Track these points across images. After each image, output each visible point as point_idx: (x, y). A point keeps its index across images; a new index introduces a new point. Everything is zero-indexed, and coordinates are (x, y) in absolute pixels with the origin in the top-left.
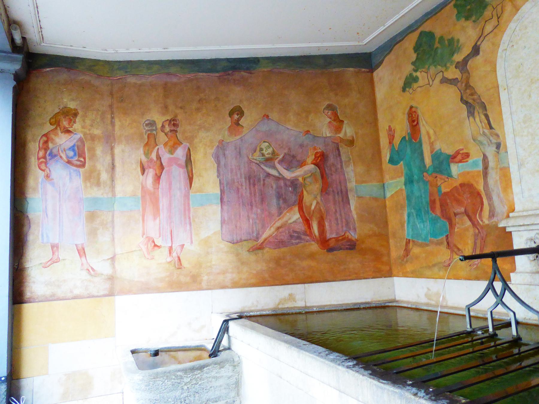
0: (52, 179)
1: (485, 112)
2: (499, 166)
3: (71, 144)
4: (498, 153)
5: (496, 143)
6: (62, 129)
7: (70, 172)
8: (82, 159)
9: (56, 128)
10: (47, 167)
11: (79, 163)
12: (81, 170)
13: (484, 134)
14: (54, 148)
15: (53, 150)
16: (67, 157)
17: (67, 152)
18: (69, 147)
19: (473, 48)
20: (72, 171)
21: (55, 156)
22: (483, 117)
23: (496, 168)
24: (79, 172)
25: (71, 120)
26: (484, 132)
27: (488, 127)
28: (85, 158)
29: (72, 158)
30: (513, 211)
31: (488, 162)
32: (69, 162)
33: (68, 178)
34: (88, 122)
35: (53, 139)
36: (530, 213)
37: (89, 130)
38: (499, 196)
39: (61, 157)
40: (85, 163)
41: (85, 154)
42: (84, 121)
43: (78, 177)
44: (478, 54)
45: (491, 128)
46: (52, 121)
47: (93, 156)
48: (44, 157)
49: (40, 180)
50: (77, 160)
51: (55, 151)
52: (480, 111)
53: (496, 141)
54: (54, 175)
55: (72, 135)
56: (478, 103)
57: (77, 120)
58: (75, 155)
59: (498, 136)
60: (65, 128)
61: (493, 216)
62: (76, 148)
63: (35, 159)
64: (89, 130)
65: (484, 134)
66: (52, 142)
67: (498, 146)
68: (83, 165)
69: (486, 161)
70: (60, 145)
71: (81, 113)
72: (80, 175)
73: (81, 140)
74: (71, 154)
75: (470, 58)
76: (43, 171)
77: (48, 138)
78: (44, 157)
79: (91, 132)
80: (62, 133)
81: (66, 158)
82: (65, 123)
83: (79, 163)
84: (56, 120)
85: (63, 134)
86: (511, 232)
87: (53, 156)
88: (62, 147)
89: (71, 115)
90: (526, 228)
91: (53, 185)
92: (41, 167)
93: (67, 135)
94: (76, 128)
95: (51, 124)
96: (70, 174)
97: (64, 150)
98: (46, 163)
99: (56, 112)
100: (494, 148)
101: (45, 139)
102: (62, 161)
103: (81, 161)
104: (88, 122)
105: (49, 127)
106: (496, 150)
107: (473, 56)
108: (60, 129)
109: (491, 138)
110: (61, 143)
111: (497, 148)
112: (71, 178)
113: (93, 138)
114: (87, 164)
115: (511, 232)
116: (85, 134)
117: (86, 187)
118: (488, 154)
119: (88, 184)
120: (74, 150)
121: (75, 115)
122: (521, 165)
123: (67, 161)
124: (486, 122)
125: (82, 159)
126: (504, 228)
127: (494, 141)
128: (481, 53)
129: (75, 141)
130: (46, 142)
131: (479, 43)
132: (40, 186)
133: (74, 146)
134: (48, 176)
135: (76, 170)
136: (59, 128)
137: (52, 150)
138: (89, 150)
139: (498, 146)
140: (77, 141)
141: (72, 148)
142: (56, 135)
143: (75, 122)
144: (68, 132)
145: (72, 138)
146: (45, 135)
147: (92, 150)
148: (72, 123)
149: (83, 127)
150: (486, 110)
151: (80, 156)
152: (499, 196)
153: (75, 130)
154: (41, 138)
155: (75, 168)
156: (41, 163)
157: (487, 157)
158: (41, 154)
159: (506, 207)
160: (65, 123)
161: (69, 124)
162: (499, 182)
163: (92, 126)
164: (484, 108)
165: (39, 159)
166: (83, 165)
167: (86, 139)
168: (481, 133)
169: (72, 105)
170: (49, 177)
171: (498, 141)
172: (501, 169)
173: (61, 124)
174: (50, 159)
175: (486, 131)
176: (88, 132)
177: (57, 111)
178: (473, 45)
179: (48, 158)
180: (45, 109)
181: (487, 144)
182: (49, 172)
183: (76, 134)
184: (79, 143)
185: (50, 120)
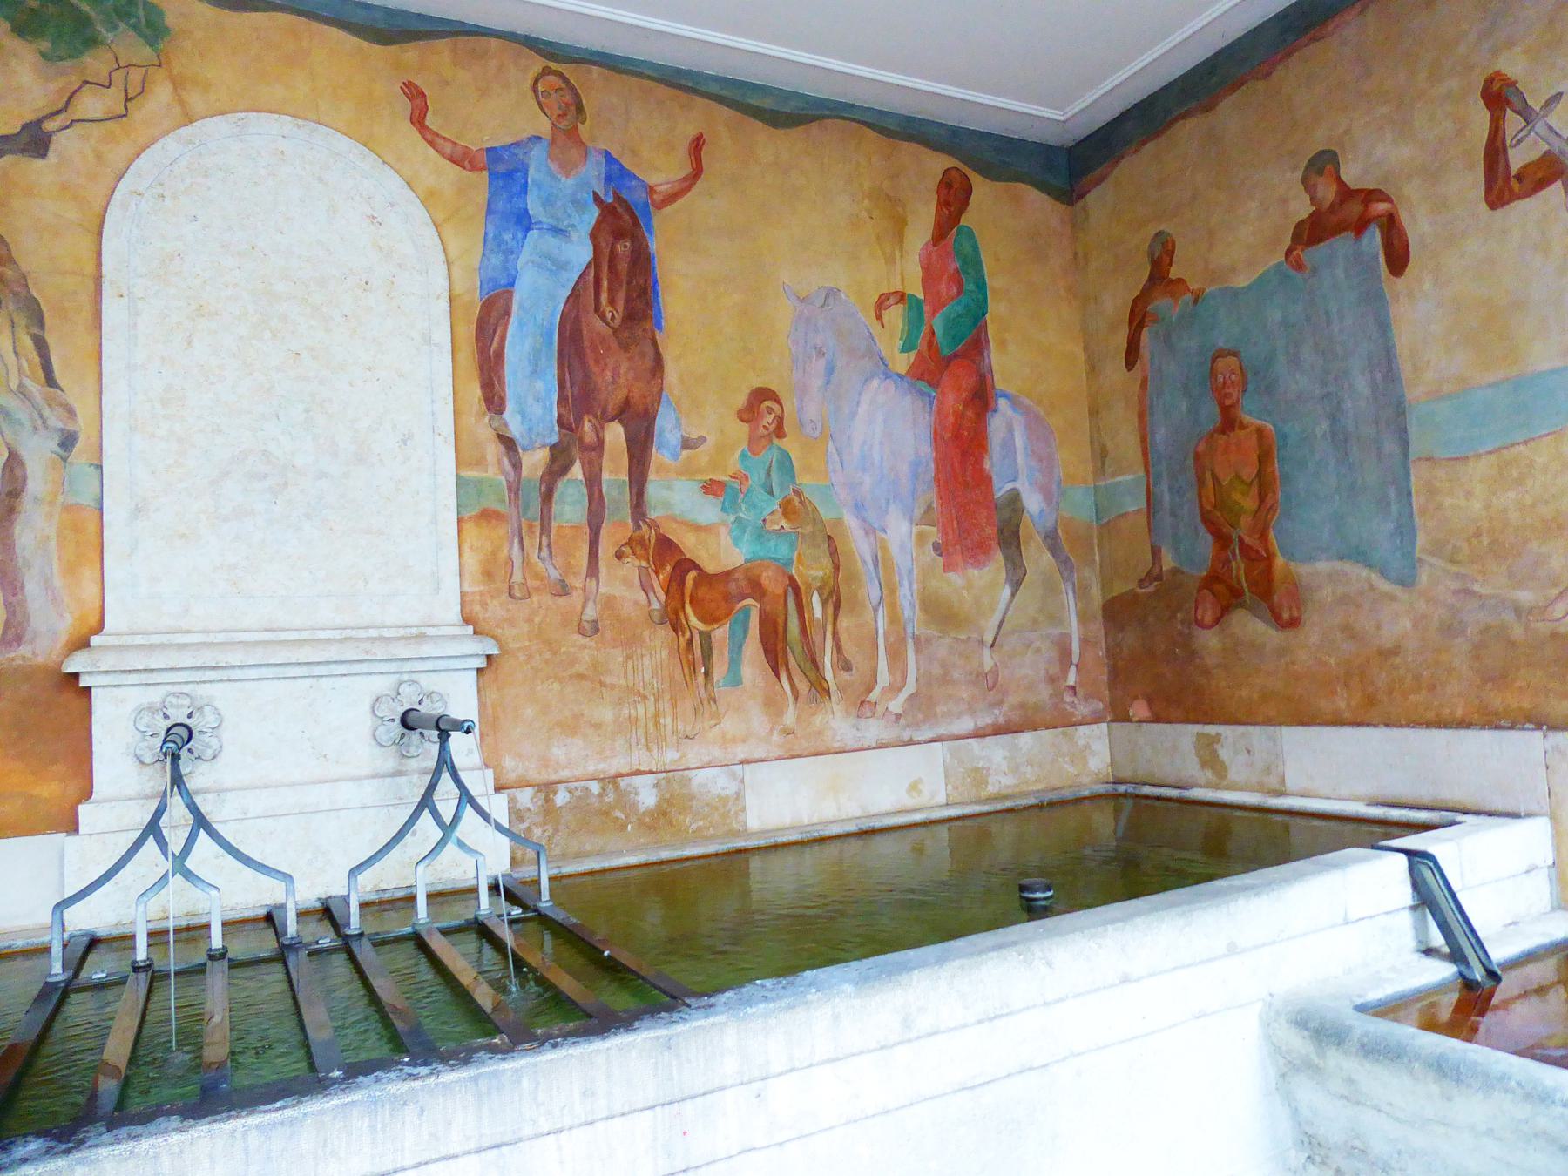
1: (35, 330)
2: (61, 499)
4: (65, 460)
5: (62, 430)
13: (22, 391)
19: (25, 127)
22: (28, 343)
23: (51, 503)
26: (21, 385)
27: (41, 374)
30: (99, 628)
31: (25, 479)
36: (155, 639)
38: (47, 584)
44: (43, 155)
45: (50, 381)
52: (21, 321)
53: (60, 425)
56: (15, 294)
59: (71, 412)
61: (19, 639)
65: (22, 391)
67: (68, 441)
69: (18, 472)
75: (12, 152)
86: (88, 689)
90: (144, 678)
100: (53, 444)
106: (58, 449)
107: (23, 151)
109: (47, 412)
111: (62, 445)
115: (88, 690)
118: (25, 454)
122: (138, 511)
124: (37, 359)
126: (76, 676)
127: (55, 420)
128: (51, 154)
131: (49, 126)
139: (68, 441)
150: (41, 324)
152: (47, 584)
157: (21, 464)
159: (69, 620)
162: (53, 543)
164: (38, 319)
168: (14, 386)
171: (71, 427)
172: (67, 508)
175: (35, 387)
178: (30, 117)
181: (28, 424)
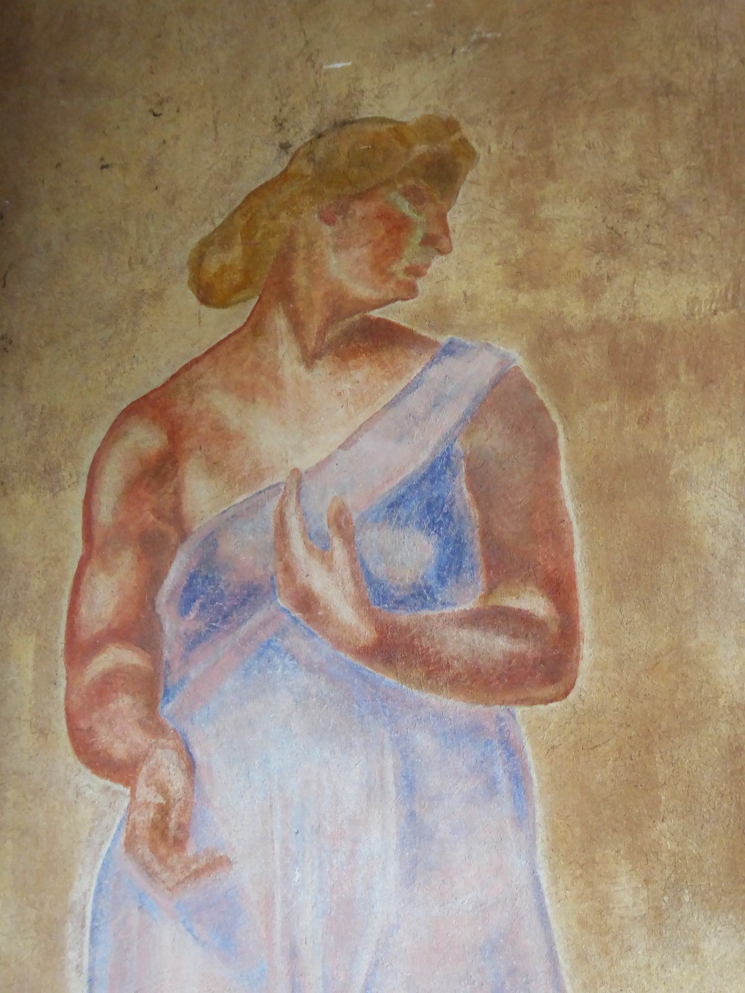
0: (217, 863)
3: (409, 457)
6: (315, 323)
7: (405, 753)
8: (535, 603)
9: (256, 326)
10: (154, 726)
11: (499, 645)
12: (527, 720)
14: (232, 518)
15: (228, 546)
16: (373, 592)
17: (374, 538)
18: (388, 490)
20: (424, 741)
21: (251, 595)
24: (511, 750)
25: (398, 226)
28: (560, 590)
29: (421, 595)
32: (393, 649)
33: (381, 837)
34: (569, 215)
35: (223, 436)
37: (590, 290)
39: (307, 603)
40: (568, 634)
41: (555, 533)
42: (526, 213)
43: (504, 807)
46: (213, 264)
47: (655, 550)
48: (137, 628)
49: (84, 886)
50: (473, 620)
51: (246, 550)
54: (233, 812)
55: (415, 365)
57: (457, 218)
58: (451, 565)
60: (339, 306)
62: (460, 491)
63: (43, 652)
64: (590, 290)
66: (213, 467)
68: (548, 666)
70: (298, 478)
71: (489, 146)
72: (519, 779)
73: (509, 403)
74: (412, 553)
76: (121, 771)
77: (175, 433)
78: (137, 628)
79: (610, 305)
80: (310, 359)
81: (362, 603)
82: (343, 267)
83: (499, 645)
84: (253, 256)
85: (323, 368)
87: (222, 600)
88: (320, 503)
89: (400, 180)
91: (222, 928)
92: (104, 737)
93: (362, 373)
94: (454, 289)
95: (207, 294)
96: (409, 786)
97: (341, 522)
98: (151, 688)
99: (249, 182)
101: (146, 438)
102: (321, 649)
103: (523, 623)
104: (569, 215)
105: (184, 327)
108: (297, 326)
110: (305, 462)
112: (415, 831)
113: (635, 364)
114: (588, 653)
116: (546, 339)
117: (597, 923)
119: (626, 894)
120: (436, 516)
121: (442, 172)
123: (366, 634)
125: (535, 603)
129: (448, 418)
130: (160, 472)
132: (77, 953)
133: (437, 470)
134: (165, 835)
135: (476, 730)
136: (280, 322)
137: (211, 541)
138: (601, 492)
140: (473, 419)
141: (421, 500)
142: (258, 386)
143: (437, 242)
144: (372, 338)
145: (415, 402)
146: (154, 406)
147: (636, 484)
148: (411, 254)
149: (523, 275)
151: (503, 565)
153: (441, 315)
154: (115, 432)
155: (456, 707)
156: (106, 686)
158: (105, 597)
160: (343, 267)
161: (380, 267)
163: (613, 246)
165: (78, 651)
166: (548, 666)
167: (559, 382)
169: (404, 96)
170: (179, 843)
173: (300, 278)
174: (195, 641)
176: (576, 311)
177: (263, 164)
179: (172, 625)
180: (150, 172)
182: (177, 782)
183: (450, 350)
184: (493, 440)
185: (198, 262)
